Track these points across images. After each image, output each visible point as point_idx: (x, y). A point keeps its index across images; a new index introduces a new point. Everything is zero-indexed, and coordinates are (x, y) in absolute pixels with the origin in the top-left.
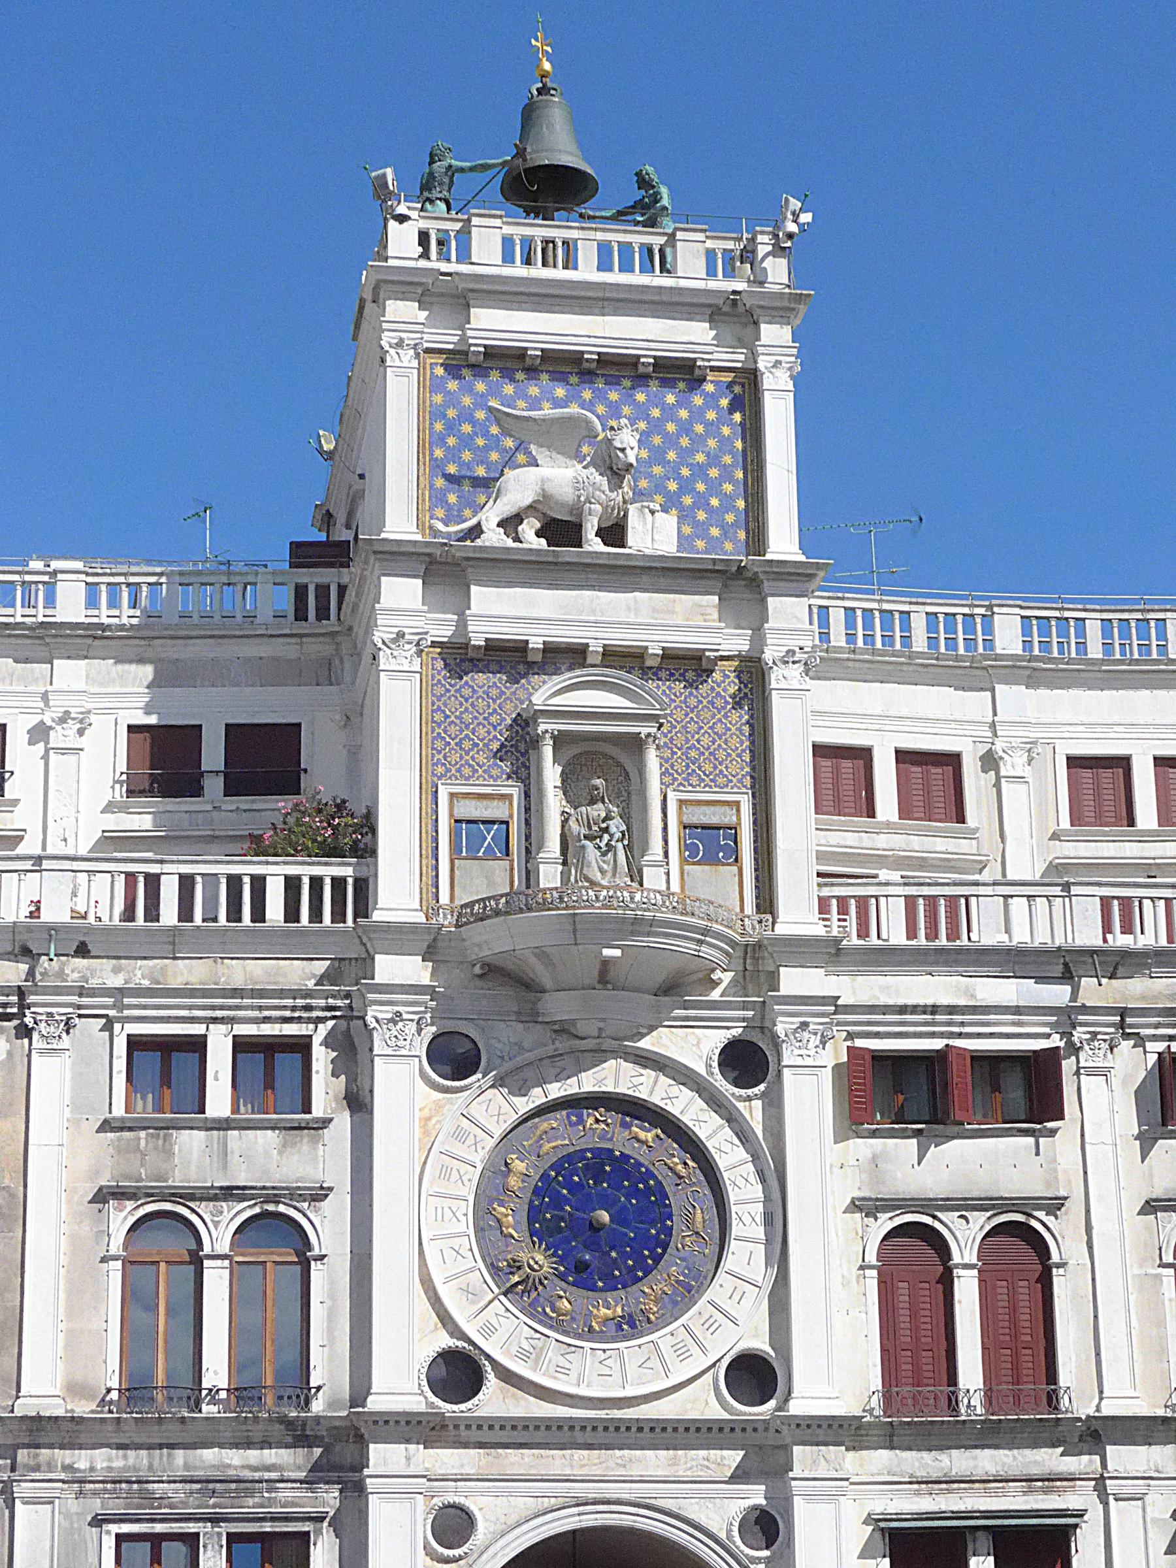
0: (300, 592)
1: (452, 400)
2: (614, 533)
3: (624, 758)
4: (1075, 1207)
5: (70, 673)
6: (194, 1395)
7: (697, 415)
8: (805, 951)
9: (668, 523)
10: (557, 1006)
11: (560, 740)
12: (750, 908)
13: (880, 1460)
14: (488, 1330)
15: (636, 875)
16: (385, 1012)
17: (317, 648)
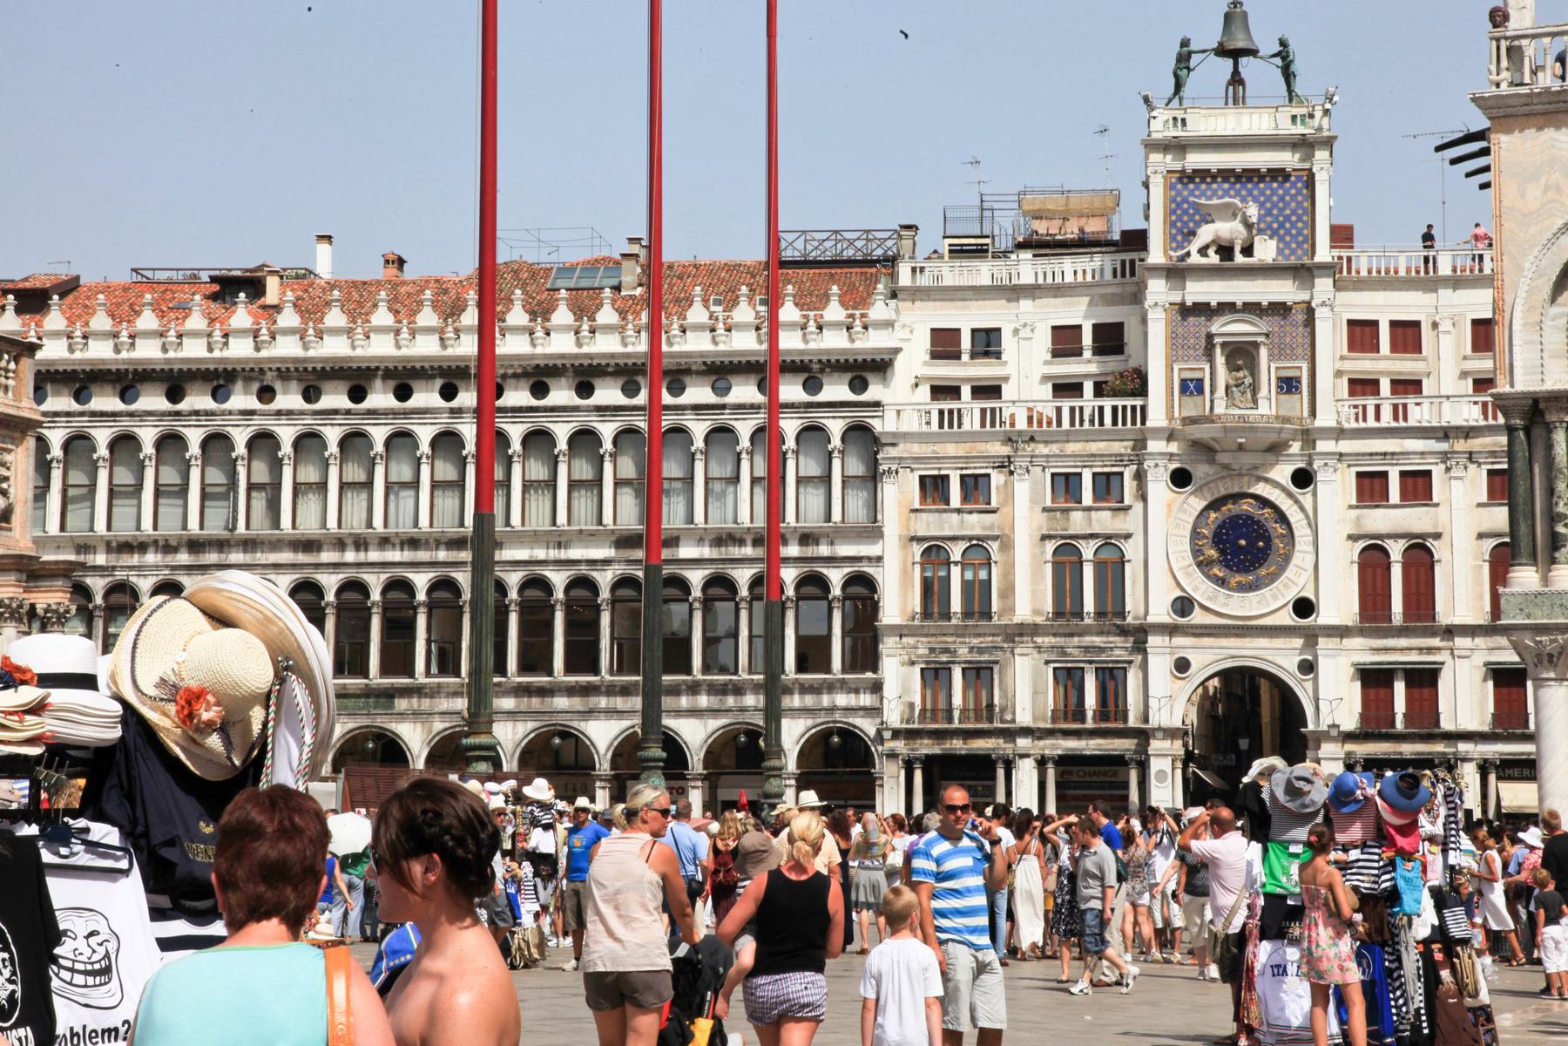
0: (1123, 262)
1: (1179, 193)
2: (1248, 251)
3: (1251, 348)
4: (1445, 537)
5: (1026, 304)
6: (1079, 614)
7: (1287, 192)
8: (1327, 433)
9: (1273, 244)
10: (1223, 458)
11: (1224, 345)
12: (1306, 414)
13: (1357, 642)
14: (1196, 589)
15: (1255, 401)
16: (1152, 463)
17: (1131, 289)
